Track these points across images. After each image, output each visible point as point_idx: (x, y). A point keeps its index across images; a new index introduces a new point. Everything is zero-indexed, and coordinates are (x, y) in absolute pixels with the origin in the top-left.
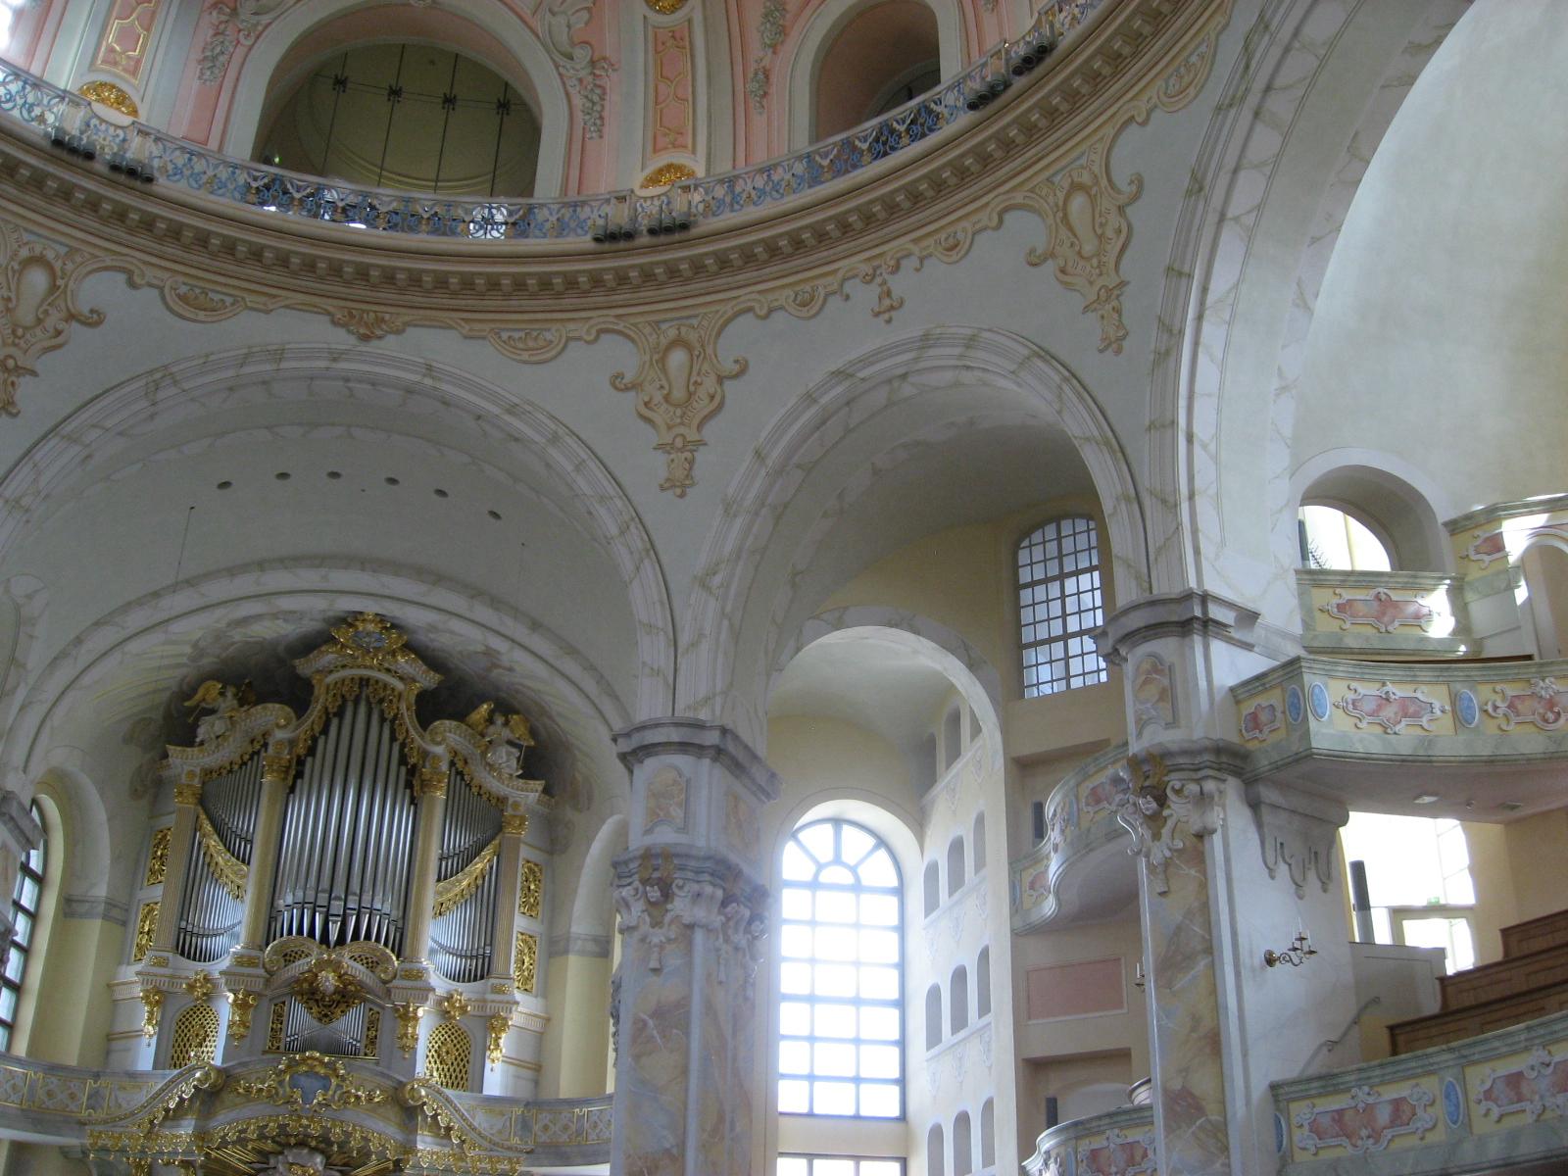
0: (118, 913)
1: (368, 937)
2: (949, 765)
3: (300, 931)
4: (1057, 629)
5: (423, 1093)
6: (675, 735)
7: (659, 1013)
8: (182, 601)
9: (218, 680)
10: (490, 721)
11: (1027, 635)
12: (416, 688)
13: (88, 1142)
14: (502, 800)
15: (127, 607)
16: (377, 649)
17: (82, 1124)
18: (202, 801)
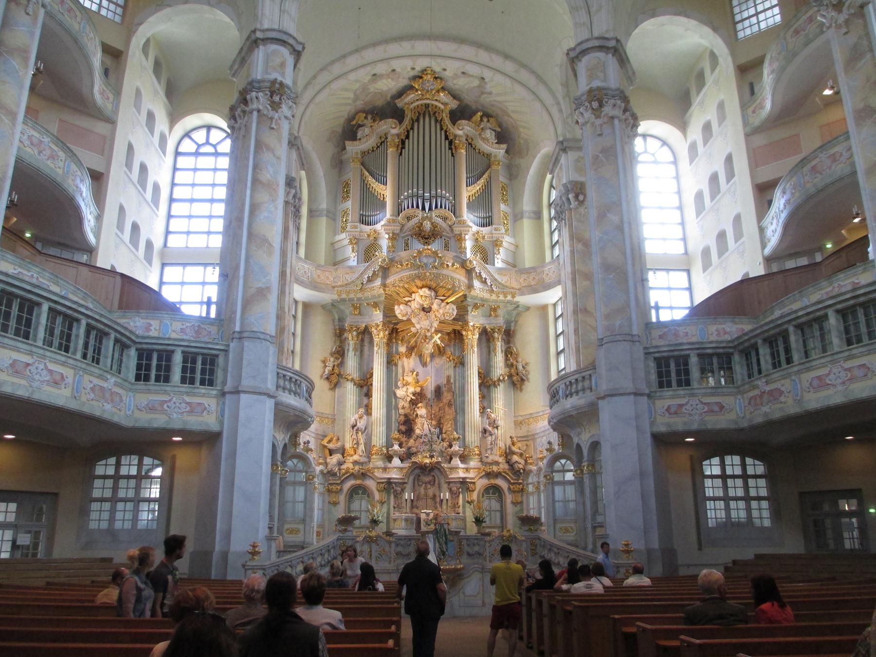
0: (332, 216)
1: (441, 207)
2: (698, 93)
3: (413, 207)
4: (752, 11)
5: (475, 262)
6: (597, 43)
7: (604, 151)
8: (352, 61)
9: (364, 112)
10: (481, 120)
11: (738, 18)
12: (449, 107)
13: (335, 297)
14: (488, 156)
15: (333, 62)
16: (432, 90)
17: (334, 287)
18: (362, 164)
